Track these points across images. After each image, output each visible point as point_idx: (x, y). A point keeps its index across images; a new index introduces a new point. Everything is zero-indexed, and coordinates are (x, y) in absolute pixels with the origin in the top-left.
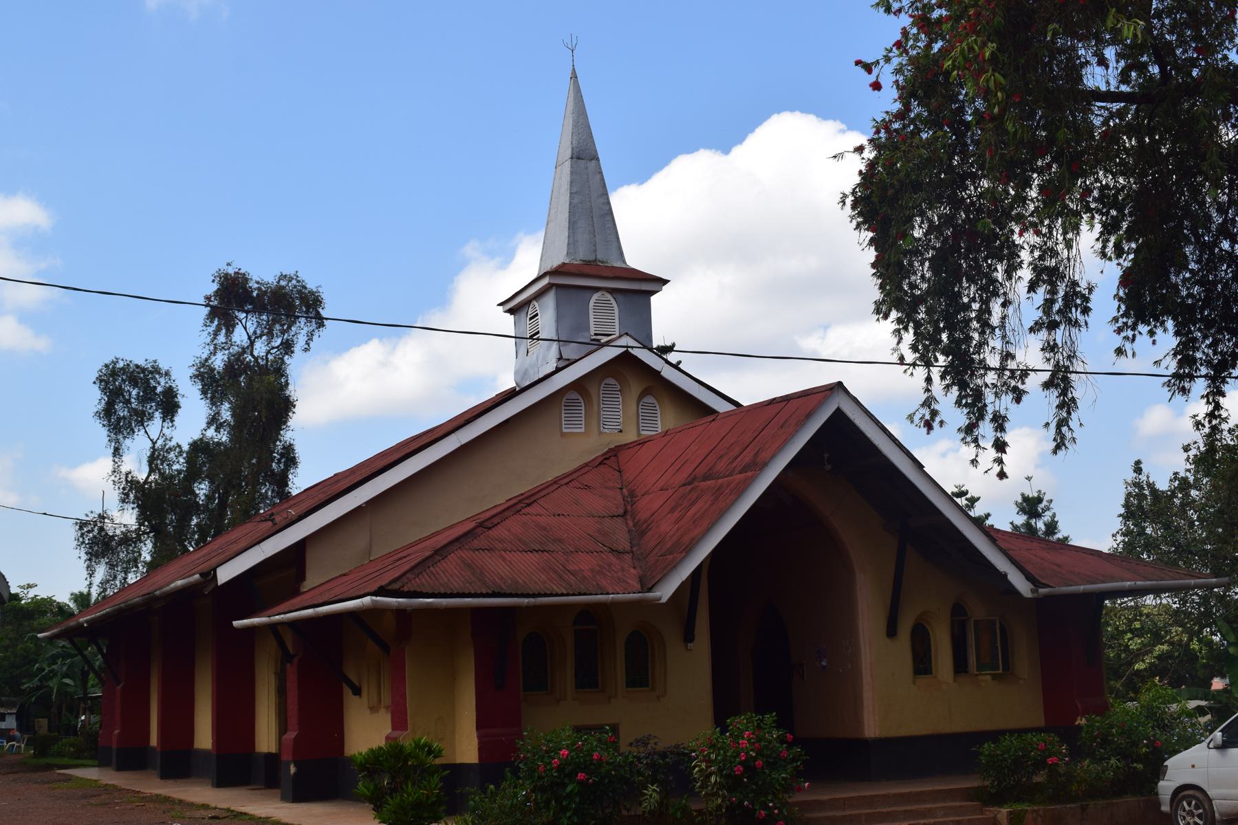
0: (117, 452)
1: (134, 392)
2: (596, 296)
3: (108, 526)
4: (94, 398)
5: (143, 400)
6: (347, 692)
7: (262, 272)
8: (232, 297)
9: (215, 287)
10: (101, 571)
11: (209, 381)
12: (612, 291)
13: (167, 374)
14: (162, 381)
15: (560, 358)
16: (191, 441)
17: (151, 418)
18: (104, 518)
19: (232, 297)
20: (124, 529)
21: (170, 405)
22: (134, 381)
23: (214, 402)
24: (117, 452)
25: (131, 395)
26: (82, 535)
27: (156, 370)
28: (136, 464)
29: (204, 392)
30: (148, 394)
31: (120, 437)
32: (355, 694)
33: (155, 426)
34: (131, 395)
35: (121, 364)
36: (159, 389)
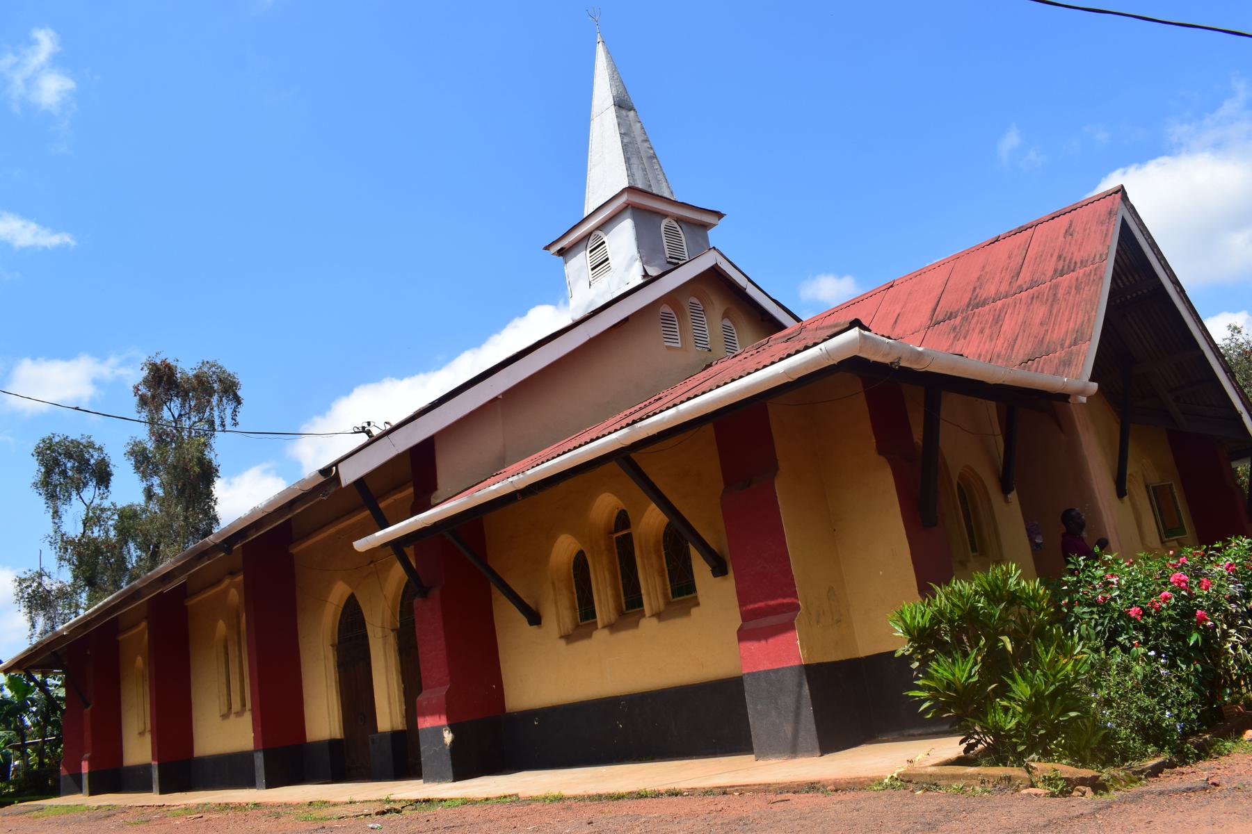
0: (56, 513)
1: (69, 465)
2: (664, 222)
3: (46, 581)
4: (34, 469)
5: (79, 470)
6: (508, 618)
7: (187, 366)
8: (162, 381)
9: (145, 373)
10: (41, 622)
11: (142, 460)
12: (679, 220)
13: (100, 449)
14: (96, 455)
15: (646, 275)
16: (170, 361)
17: (85, 485)
18: (40, 576)
19: (162, 381)
20: (59, 585)
21: (103, 476)
22: (69, 456)
23: (145, 476)
24: (56, 513)
25: (67, 466)
26: (21, 590)
27: (91, 445)
28: (73, 527)
29: (137, 468)
30: (83, 464)
31: (59, 503)
32: (531, 624)
33: (90, 493)
34: (67, 466)
35: (57, 439)
36: (92, 461)
